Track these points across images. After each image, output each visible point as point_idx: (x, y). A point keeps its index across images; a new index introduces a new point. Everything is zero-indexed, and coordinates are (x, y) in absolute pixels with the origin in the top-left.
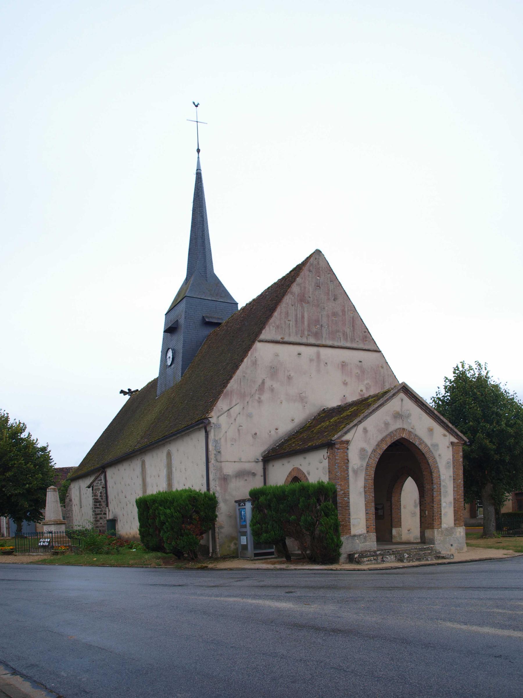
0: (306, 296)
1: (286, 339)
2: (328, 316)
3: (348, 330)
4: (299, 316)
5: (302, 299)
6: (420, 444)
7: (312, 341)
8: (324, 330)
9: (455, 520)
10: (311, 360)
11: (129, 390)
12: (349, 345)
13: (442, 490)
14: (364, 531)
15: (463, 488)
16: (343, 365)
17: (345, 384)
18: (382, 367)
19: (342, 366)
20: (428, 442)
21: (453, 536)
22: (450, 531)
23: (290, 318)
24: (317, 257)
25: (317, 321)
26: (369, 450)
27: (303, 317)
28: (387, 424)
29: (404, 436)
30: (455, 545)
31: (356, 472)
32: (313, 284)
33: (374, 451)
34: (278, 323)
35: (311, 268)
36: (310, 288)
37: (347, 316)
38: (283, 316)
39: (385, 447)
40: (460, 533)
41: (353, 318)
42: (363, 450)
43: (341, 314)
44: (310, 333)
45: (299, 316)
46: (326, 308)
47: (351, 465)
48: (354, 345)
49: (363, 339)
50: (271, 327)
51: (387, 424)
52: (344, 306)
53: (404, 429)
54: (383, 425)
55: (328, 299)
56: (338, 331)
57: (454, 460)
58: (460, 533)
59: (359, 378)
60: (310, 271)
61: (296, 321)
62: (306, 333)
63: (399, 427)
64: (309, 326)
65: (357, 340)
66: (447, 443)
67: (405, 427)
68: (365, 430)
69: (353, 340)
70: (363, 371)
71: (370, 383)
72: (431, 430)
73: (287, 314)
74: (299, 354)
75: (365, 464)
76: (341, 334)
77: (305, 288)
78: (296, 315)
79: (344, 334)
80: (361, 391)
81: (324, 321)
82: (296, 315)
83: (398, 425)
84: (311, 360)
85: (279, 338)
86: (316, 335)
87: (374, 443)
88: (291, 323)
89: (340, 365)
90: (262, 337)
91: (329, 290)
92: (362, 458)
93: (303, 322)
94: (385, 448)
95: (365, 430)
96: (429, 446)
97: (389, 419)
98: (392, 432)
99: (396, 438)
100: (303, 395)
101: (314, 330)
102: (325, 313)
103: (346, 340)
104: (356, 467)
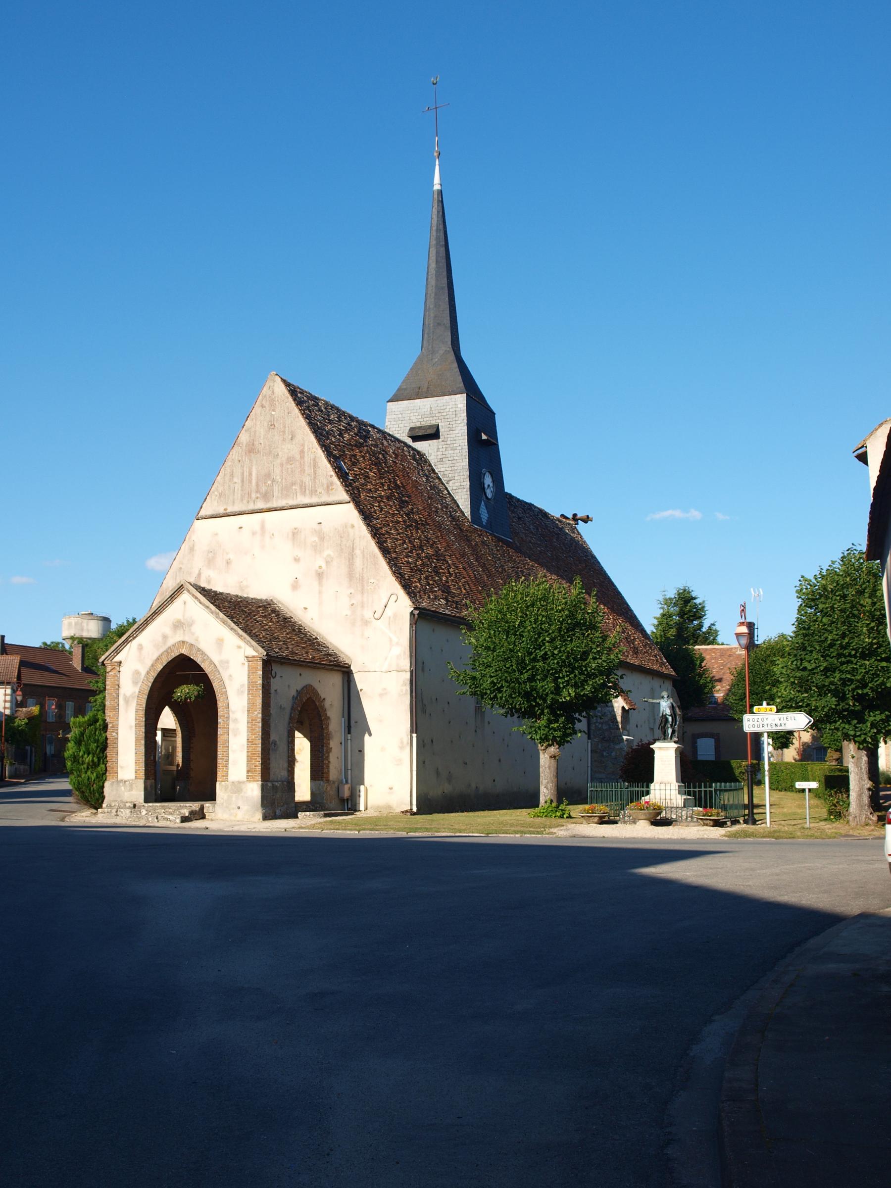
0: (256, 443)
1: (230, 510)
2: (282, 465)
3: (307, 480)
4: (246, 474)
5: (251, 450)
6: (204, 661)
7: (261, 505)
8: (276, 487)
9: (248, 771)
10: (254, 533)
11: (575, 515)
12: (307, 500)
13: (231, 726)
14: (133, 776)
15: (260, 725)
16: (295, 534)
17: (297, 560)
18: (353, 526)
19: (294, 534)
20: (215, 659)
21: (242, 794)
22: (237, 787)
23: (235, 480)
24: (271, 384)
25: (268, 476)
26: (143, 673)
27: (250, 474)
28: (165, 637)
29: (184, 651)
30: (245, 808)
31: (127, 701)
32: (266, 425)
33: (148, 673)
34: (221, 489)
35: (264, 402)
36: (261, 431)
37: (306, 459)
38: (227, 479)
39: (160, 667)
40: (252, 790)
41: (314, 460)
42: (137, 673)
43: (298, 457)
44: (258, 495)
45: (246, 474)
46: (280, 454)
47: (122, 691)
48: (314, 500)
49: (328, 487)
50: (214, 497)
51: (165, 637)
52: (303, 445)
53: (183, 642)
54: (160, 639)
55: (284, 440)
56: (293, 484)
57: (251, 684)
58: (252, 790)
59: (316, 549)
60: (263, 406)
61: (243, 481)
62: (254, 495)
63: (181, 639)
64: (257, 485)
65: (319, 490)
66: (242, 659)
67: (187, 639)
68: (140, 647)
69: (313, 492)
70: (322, 539)
71: (332, 554)
72: (220, 642)
73: (232, 475)
74: (241, 528)
75: (137, 691)
76: (296, 487)
77: (255, 432)
78: (243, 474)
79: (301, 486)
80: (320, 567)
81: (277, 474)
82: (243, 474)
83: (178, 637)
84: (254, 533)
85: (221, 511)
86: (266, 496)
87: (149, 663)
88: (236, 485)
89: (291, 534)
90: (203, 513)
91: (285, 427)
92: (135, 683)
93: (250, 482)
94: (159, 670)
95: (140, 647)
96: (217, 664)
97: (168, 631)
98: (170, 648)
99: (174, 655)
100: (245, 583)
101: (263, 489)
102: (278, 461)
103: (304, 493)
104: (128, 694)
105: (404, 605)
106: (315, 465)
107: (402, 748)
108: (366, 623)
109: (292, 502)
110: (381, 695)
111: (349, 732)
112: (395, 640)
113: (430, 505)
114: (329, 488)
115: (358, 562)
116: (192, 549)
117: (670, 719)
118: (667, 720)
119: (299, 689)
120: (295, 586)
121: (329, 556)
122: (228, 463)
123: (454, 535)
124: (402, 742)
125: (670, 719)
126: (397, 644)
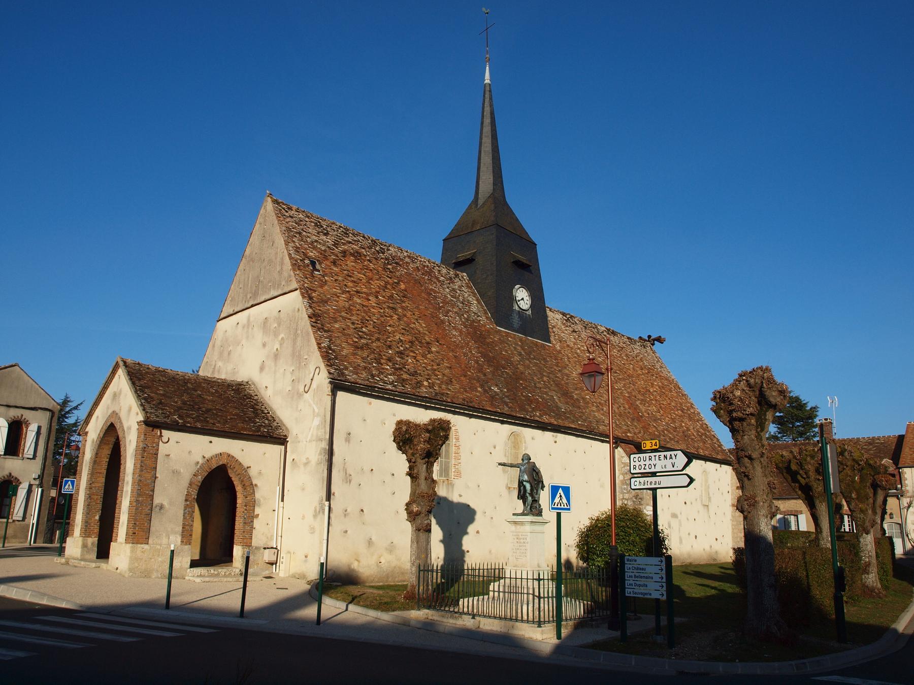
11: (649, 337)
17: (264, 345)
51: (108, 408)
103: (274, 288)
105: (323, 379)
106: (282, 263)
107: (315, 516)
108: (300, 396)
109: (268, 297)
110: (306, 464)
111: (283, 500)
112: (316, 410)
113: (440, 308)
114: (289, 281)
115: (299, 343)
116: (214, 346)
117: (528, 486)
118: (525, 487)
119: (208, 456)
120: (262, 368)
121: (282, 339)
122: (239, 273)
123: (461, 332)
124: (315, 511)
125: (528, 486)
126: (318, 415)
